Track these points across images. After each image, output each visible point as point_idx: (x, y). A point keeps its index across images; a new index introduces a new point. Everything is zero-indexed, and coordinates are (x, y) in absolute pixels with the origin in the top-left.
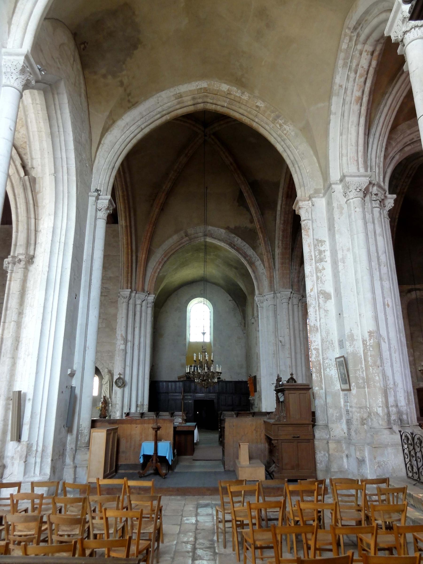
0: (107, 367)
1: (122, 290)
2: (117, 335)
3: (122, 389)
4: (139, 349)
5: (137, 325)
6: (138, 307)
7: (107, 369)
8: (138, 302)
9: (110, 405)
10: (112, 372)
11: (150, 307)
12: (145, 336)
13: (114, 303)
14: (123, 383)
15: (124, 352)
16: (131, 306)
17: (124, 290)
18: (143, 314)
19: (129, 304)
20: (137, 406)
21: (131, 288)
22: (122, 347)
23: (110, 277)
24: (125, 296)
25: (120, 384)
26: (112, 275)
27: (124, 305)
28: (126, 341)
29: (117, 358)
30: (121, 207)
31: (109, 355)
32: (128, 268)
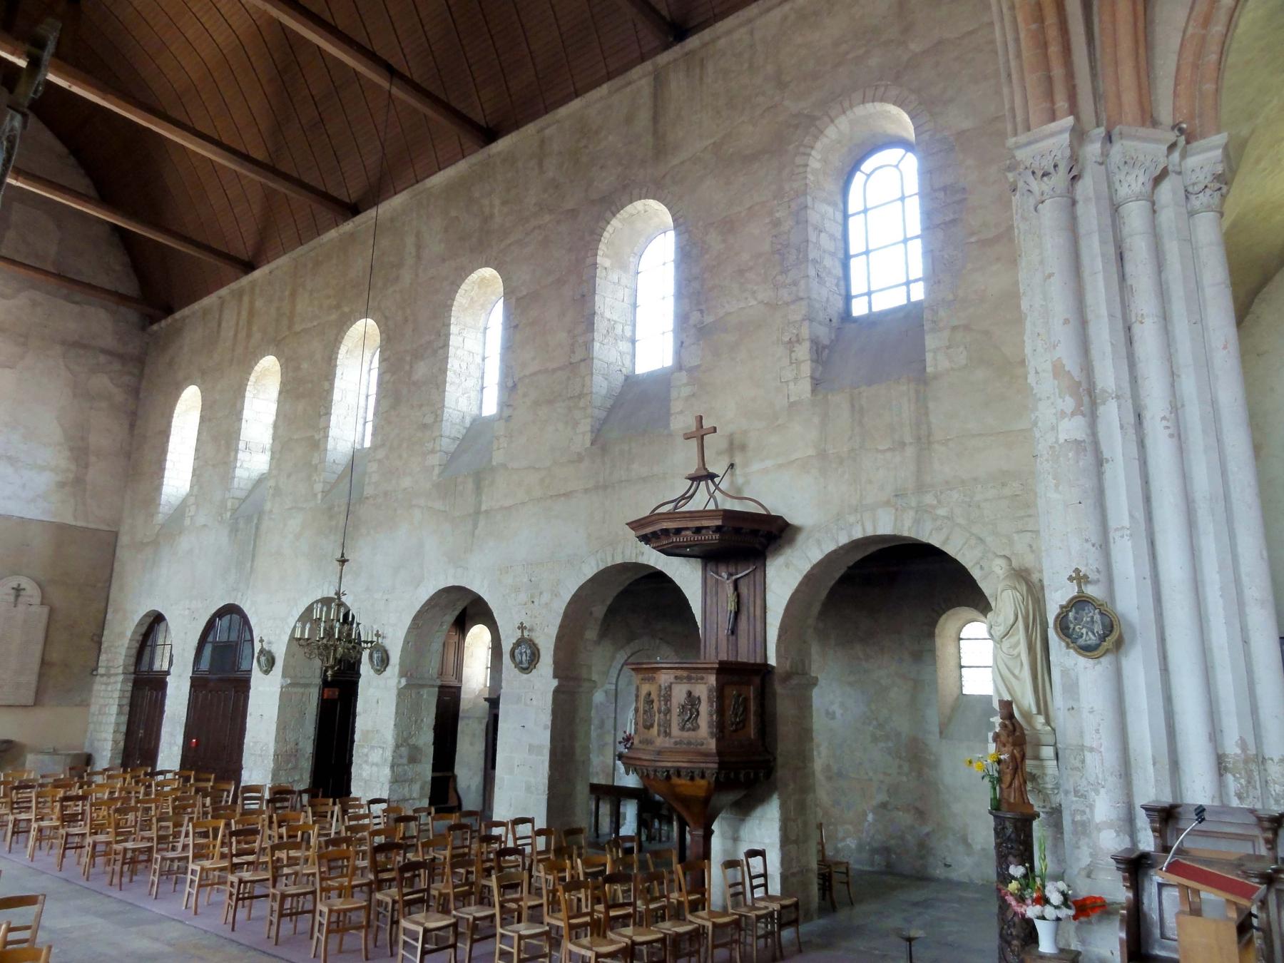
0: (1007, 553)
1: (1022, 138)
2: (1031, 379)
3: (1105, 661)
4: (1179, 436)
5: (1144, 303)
6: (1135, 216)
7: (1002, 562)
8: (1132, 184)
9: (1047, 752)
10: (1035, 577)
11: (1208, 208)
12: (1205, 364)
13: (1001, 243)
14: (1109, 627)
15: (1087, 460)
16: (1090, 216)
17: (1036, 132)
18: (1172, 249)
19: (1074, 203)
20: (1221, 765)
21: (1073, 109)
22: (1073, 428)
23: (961, 134)
24: (1047, 164)
25: (1092, 639)
26: (966, 124)
27: (1050, 215)
28: (1088, 399)
29: (1053, 495)
30: (1012, 101)
31: (1007, 491)
32: (1040, 19)
